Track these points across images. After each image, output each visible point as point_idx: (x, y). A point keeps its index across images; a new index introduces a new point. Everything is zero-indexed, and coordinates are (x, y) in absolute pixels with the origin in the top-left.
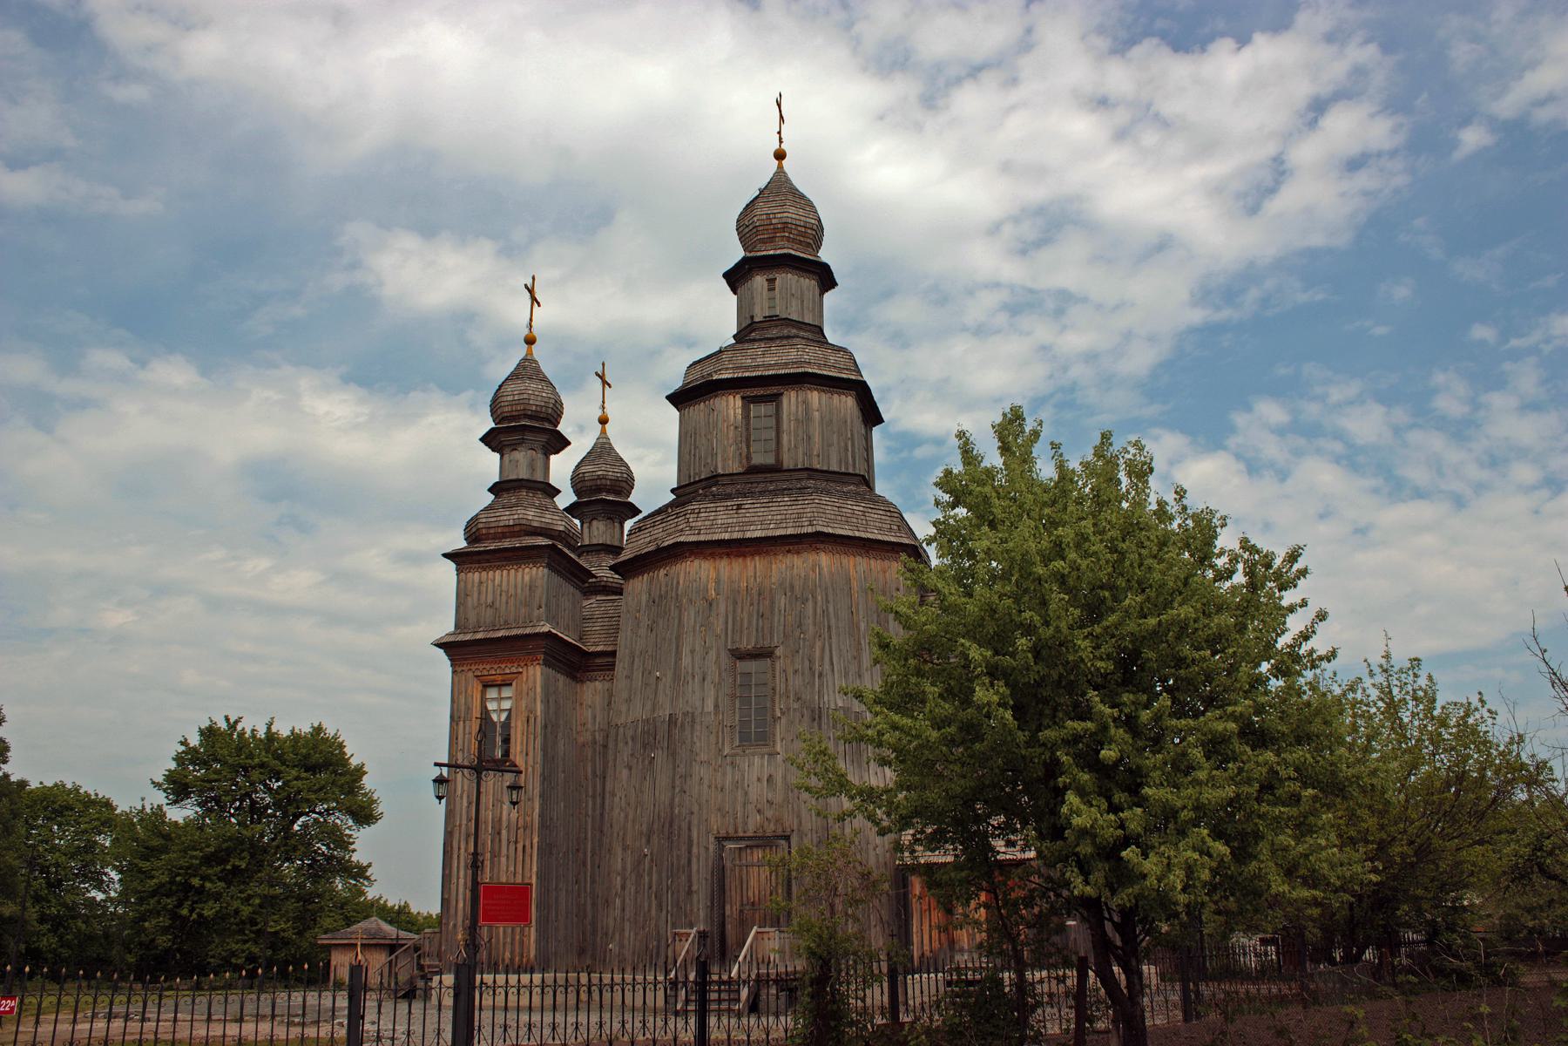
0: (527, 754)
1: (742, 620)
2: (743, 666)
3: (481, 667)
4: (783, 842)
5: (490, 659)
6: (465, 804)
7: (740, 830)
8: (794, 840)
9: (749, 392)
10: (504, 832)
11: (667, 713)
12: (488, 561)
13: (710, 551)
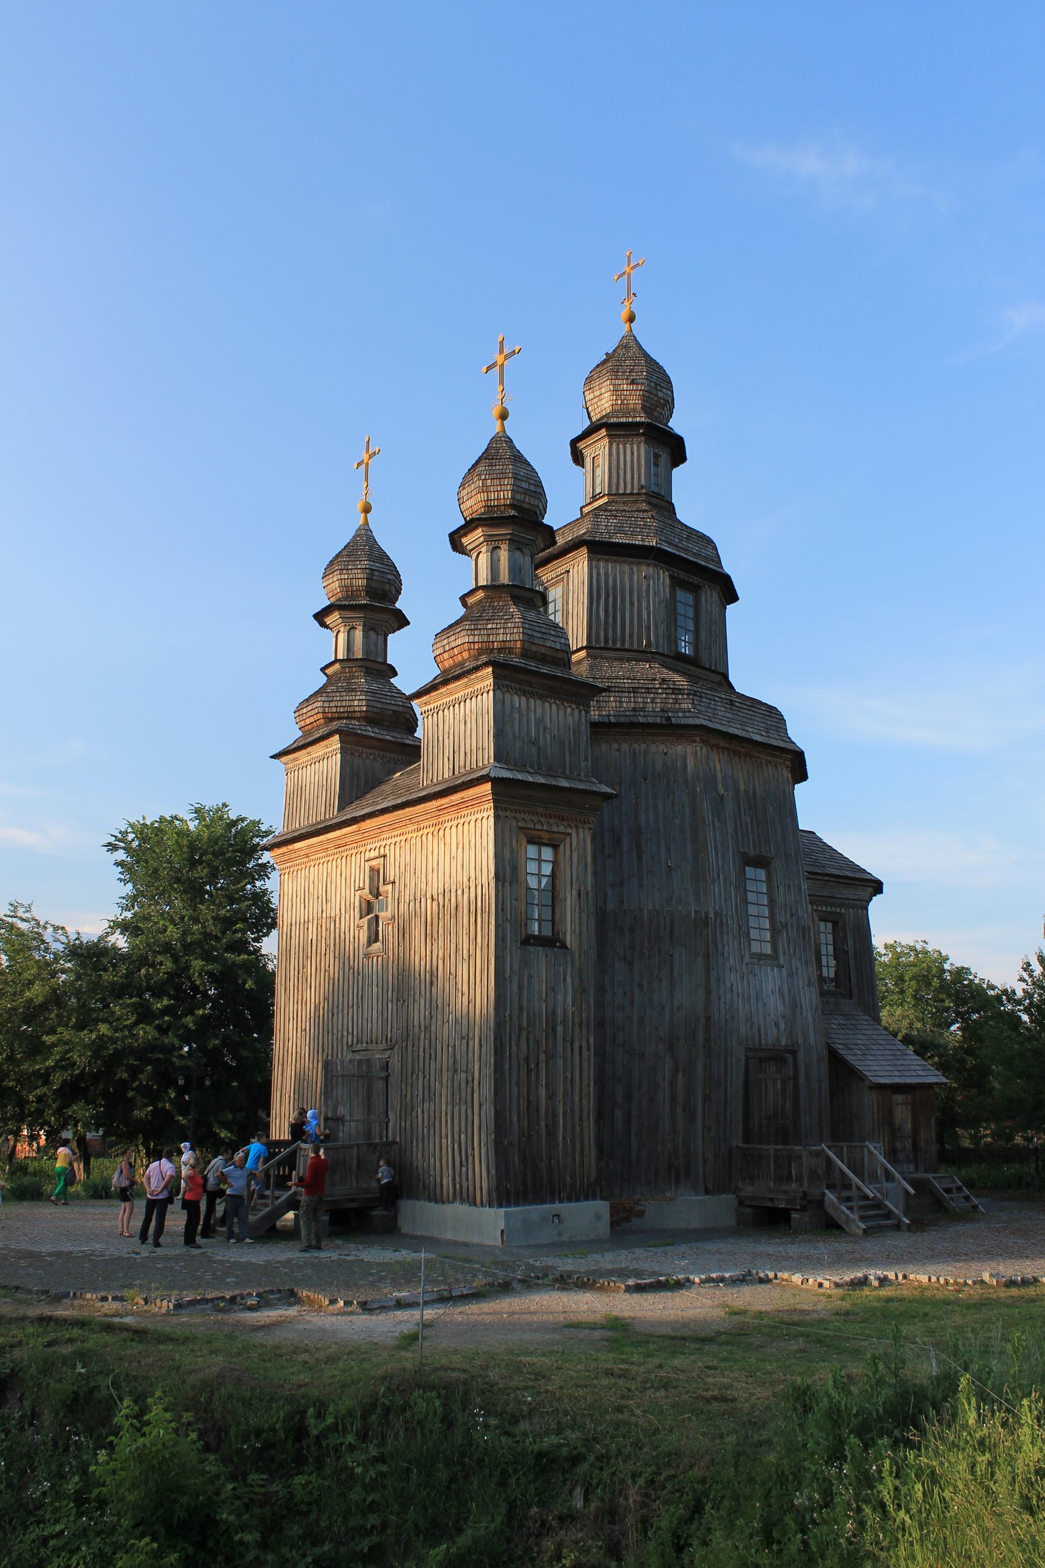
0: (580, 935)
1: (746, 823)
2: (750, 871)
3: (527, 817)
4: (789, 1056)
5: (540, 810)
6: (515, 989)
7: (763, 1042)
8: (801, 1054)
9: (677, 572)
10: (560, 1029)
11: (693, 908)
12: (530, 684)
13: (714, 741)
